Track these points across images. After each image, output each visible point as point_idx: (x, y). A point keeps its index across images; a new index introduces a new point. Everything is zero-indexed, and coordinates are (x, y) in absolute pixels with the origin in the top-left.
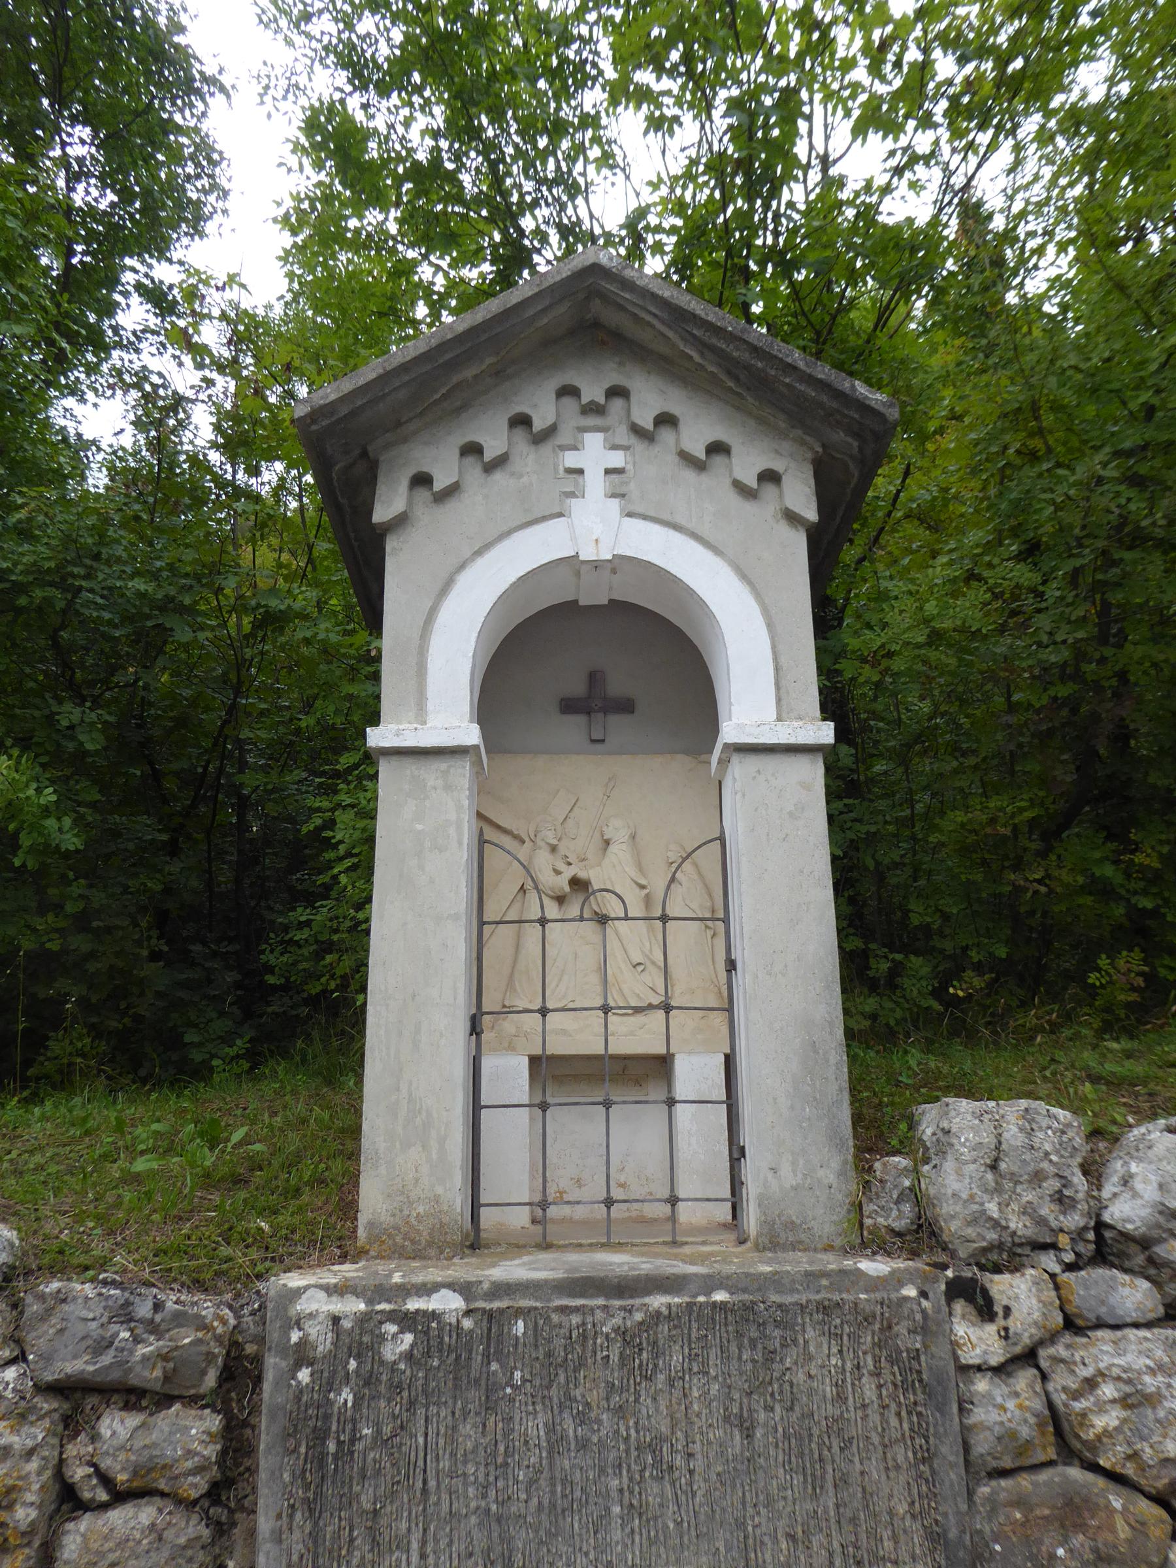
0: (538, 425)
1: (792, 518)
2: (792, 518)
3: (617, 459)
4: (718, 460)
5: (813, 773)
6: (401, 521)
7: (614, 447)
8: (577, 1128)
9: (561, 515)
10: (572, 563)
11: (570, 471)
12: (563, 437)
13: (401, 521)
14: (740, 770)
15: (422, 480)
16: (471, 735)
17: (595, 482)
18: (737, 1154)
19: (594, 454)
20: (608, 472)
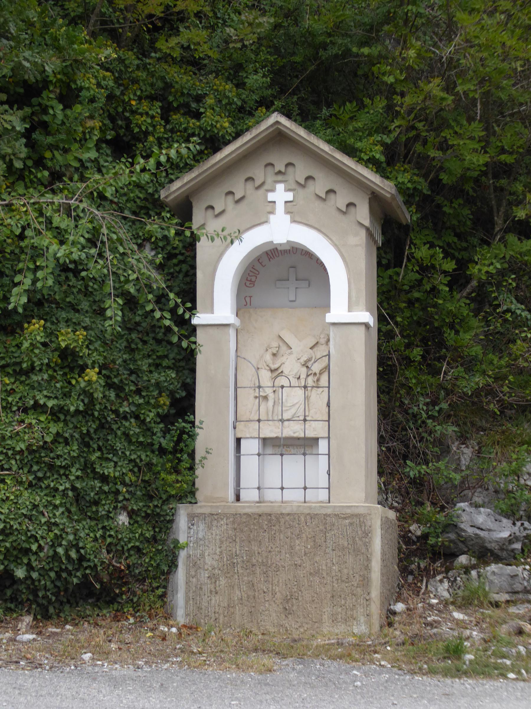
3: (290, 196)
9: (266, 222)
17: (280, 207)
19: (280, 195)
20: (286, 202)
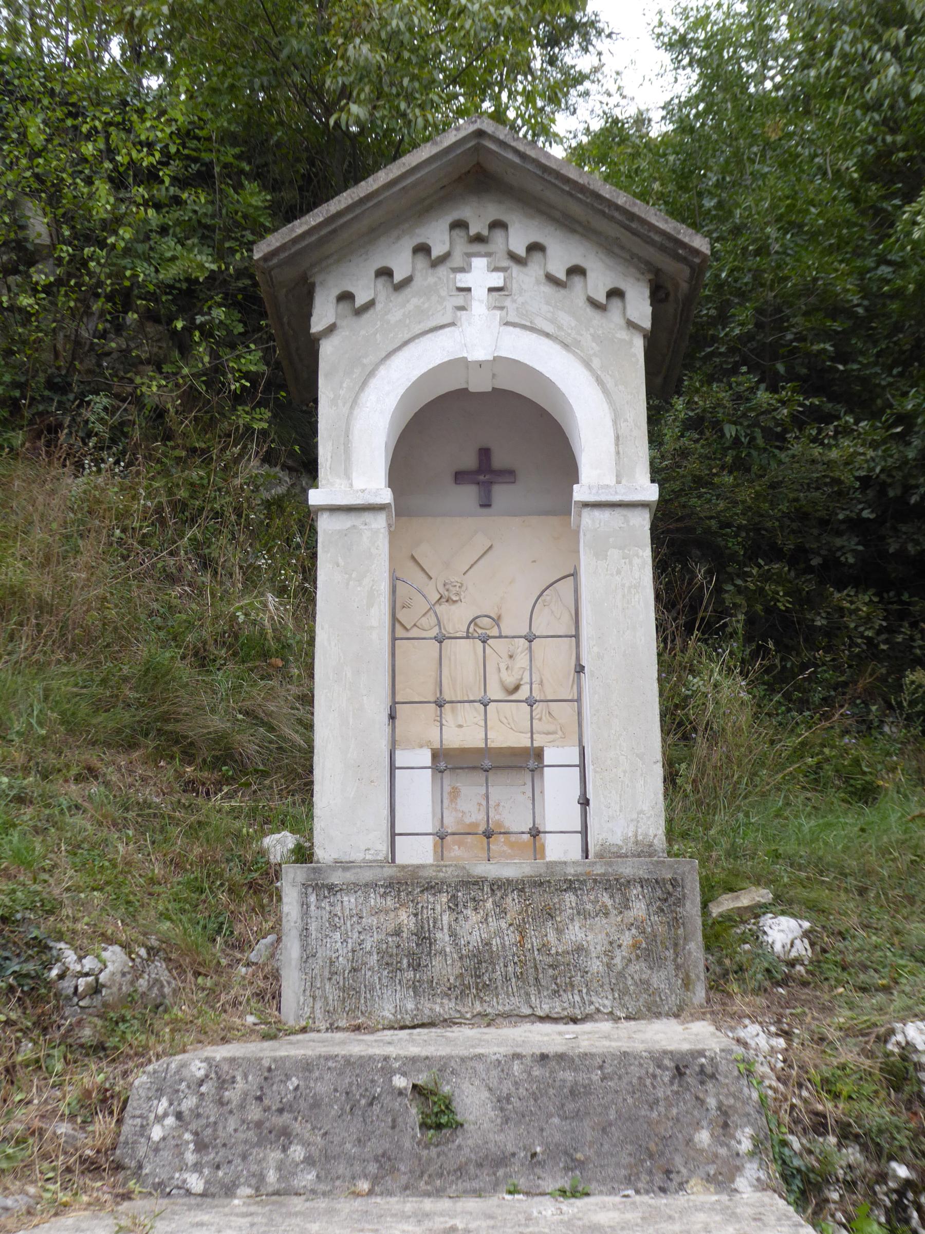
0: (436, 252)
1: (631, 325)
2: (631, 325)
3: (497, 280)
4: (577, 280)
5: (642, 522)
6: (331, 329)
7: (497, 269)
8: (470, 803)
9: (453, 324)
10: (463, 362)
11: (460, 290)
12: (457, 260)
13: (331, 329)
14: (589, 520)
15: (346, 297)
16: (386, 496)
18: (585, 802)
19: (480, 275)
20: (491, 290)
